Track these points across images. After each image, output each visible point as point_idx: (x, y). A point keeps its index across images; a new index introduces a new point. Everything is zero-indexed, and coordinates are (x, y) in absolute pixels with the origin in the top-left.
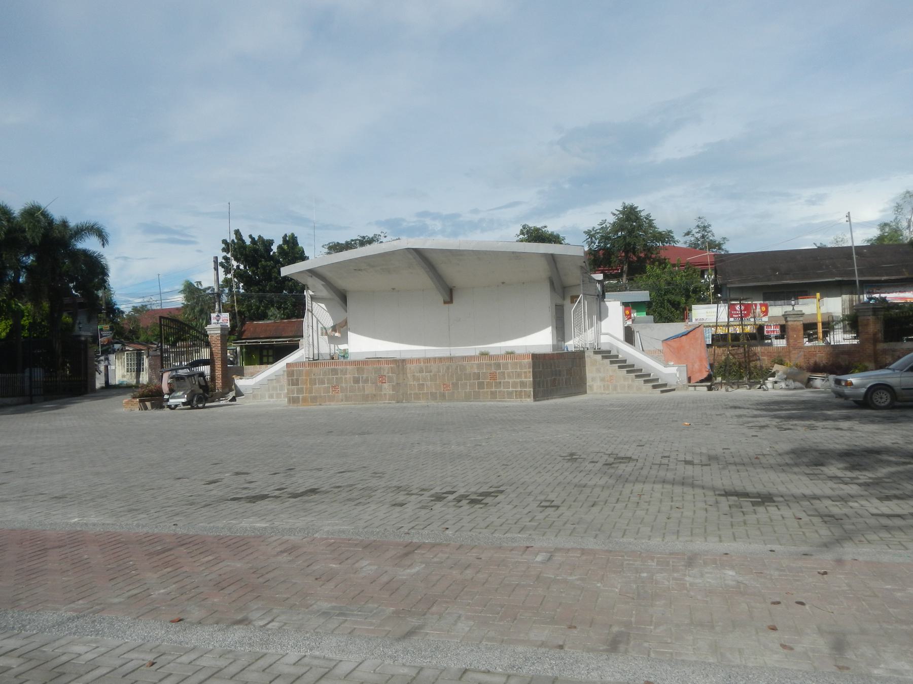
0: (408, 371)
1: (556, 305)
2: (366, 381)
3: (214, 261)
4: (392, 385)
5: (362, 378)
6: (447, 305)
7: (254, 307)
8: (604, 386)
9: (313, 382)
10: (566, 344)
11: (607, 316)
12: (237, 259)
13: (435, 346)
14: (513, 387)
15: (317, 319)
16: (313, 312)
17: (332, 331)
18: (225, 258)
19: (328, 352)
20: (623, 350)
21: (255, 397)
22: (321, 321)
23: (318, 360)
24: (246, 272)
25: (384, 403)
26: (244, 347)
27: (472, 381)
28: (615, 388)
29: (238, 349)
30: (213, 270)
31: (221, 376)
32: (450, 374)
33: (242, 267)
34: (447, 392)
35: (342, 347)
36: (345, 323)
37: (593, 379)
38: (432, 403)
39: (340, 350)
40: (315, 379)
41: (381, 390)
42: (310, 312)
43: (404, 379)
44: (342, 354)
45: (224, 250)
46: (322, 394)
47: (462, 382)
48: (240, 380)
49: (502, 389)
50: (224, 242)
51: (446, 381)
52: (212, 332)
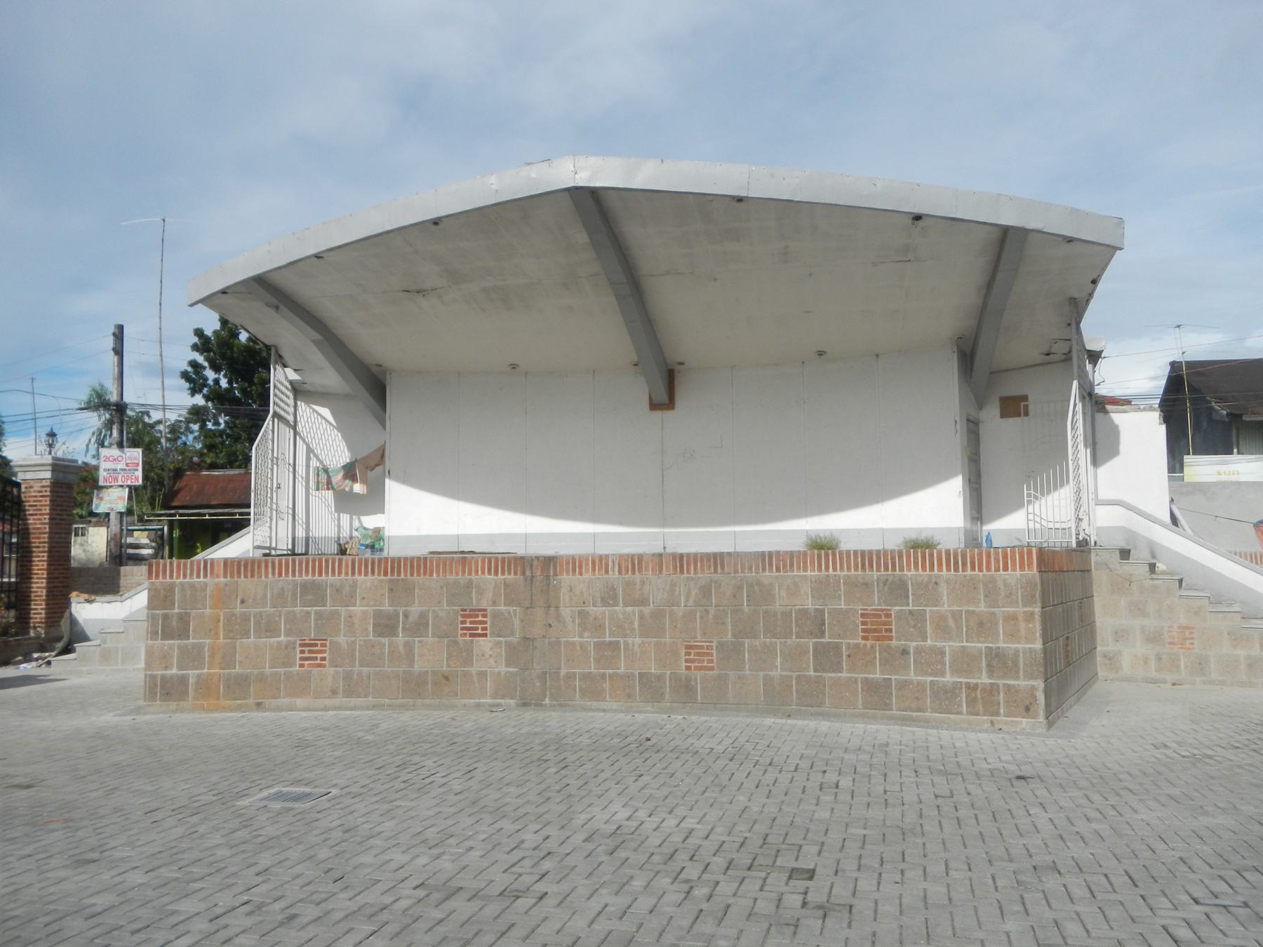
0: (564, 595)
1: (968, 420)
2: (419, 627)
3: (114, 334)
4: (508, 644)
5: (406, 616)
6: (658, 415)
7: (240, 457)
8: (1159, 658)
9: (238, 627)
10: (987, 528)
11: (1114, 451)
12: (216, 369)
13: (621, 523)
14: (957, 670)
15: (308, 445)
16: (299, 428)
17: (346, 477)
18: (194, 364)
19: (331, 532)
20: (1168, 549)
21: (106, 656)
22: (318, 451)
23: (306, 554)
24: (230, 390)
25: (478, 705)
26: (176, 524)
27: (793, 641)
28: (1200, 666)
29: (166, 528)
30: (112, 353)
31: (44, 591)
32: (712, 611)
33: (224, 383)
34: (699, 674)
35: (371, 522)
36: (379, 458)
37: (1120, 635)
38: (645, 717)
39: (365, 529)
40: (246, 618)
41: (468, 661)
42: (286, 422)
43: (550, 626)
44: (368, 542)
45: (195, 347)
46: (268, 670)
47: (757, 642)
48: (87, 605)
49: (912, 676)
50: (199, 333)
51: (699, 638)
52: (29, 476)
